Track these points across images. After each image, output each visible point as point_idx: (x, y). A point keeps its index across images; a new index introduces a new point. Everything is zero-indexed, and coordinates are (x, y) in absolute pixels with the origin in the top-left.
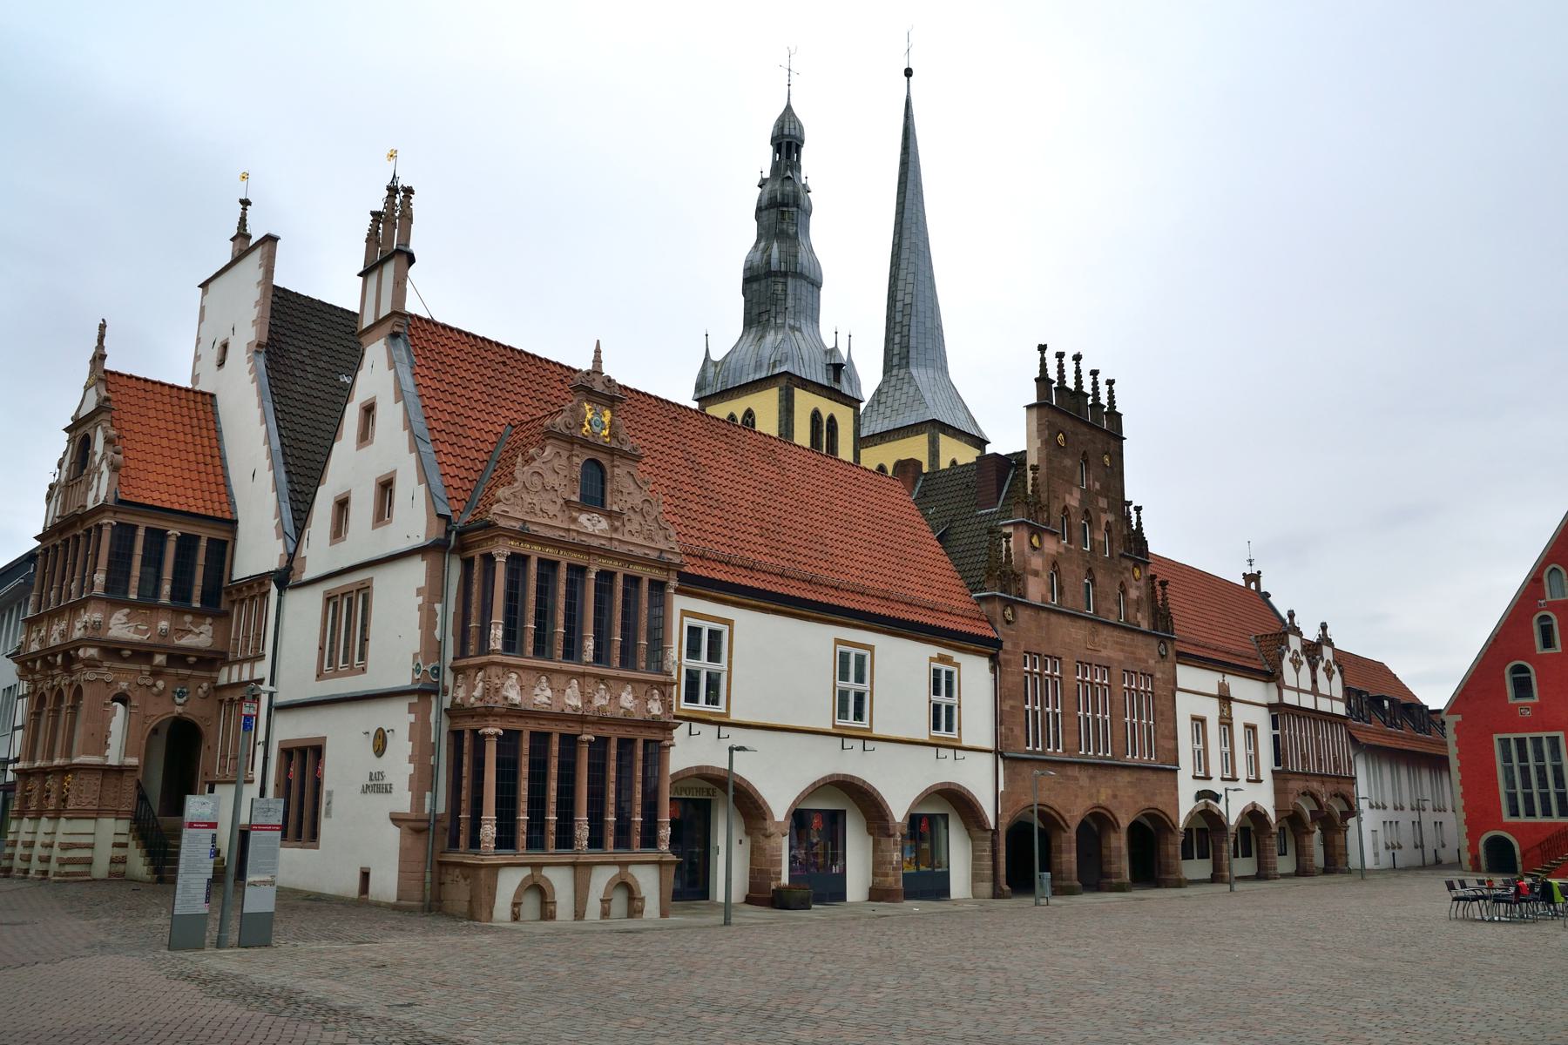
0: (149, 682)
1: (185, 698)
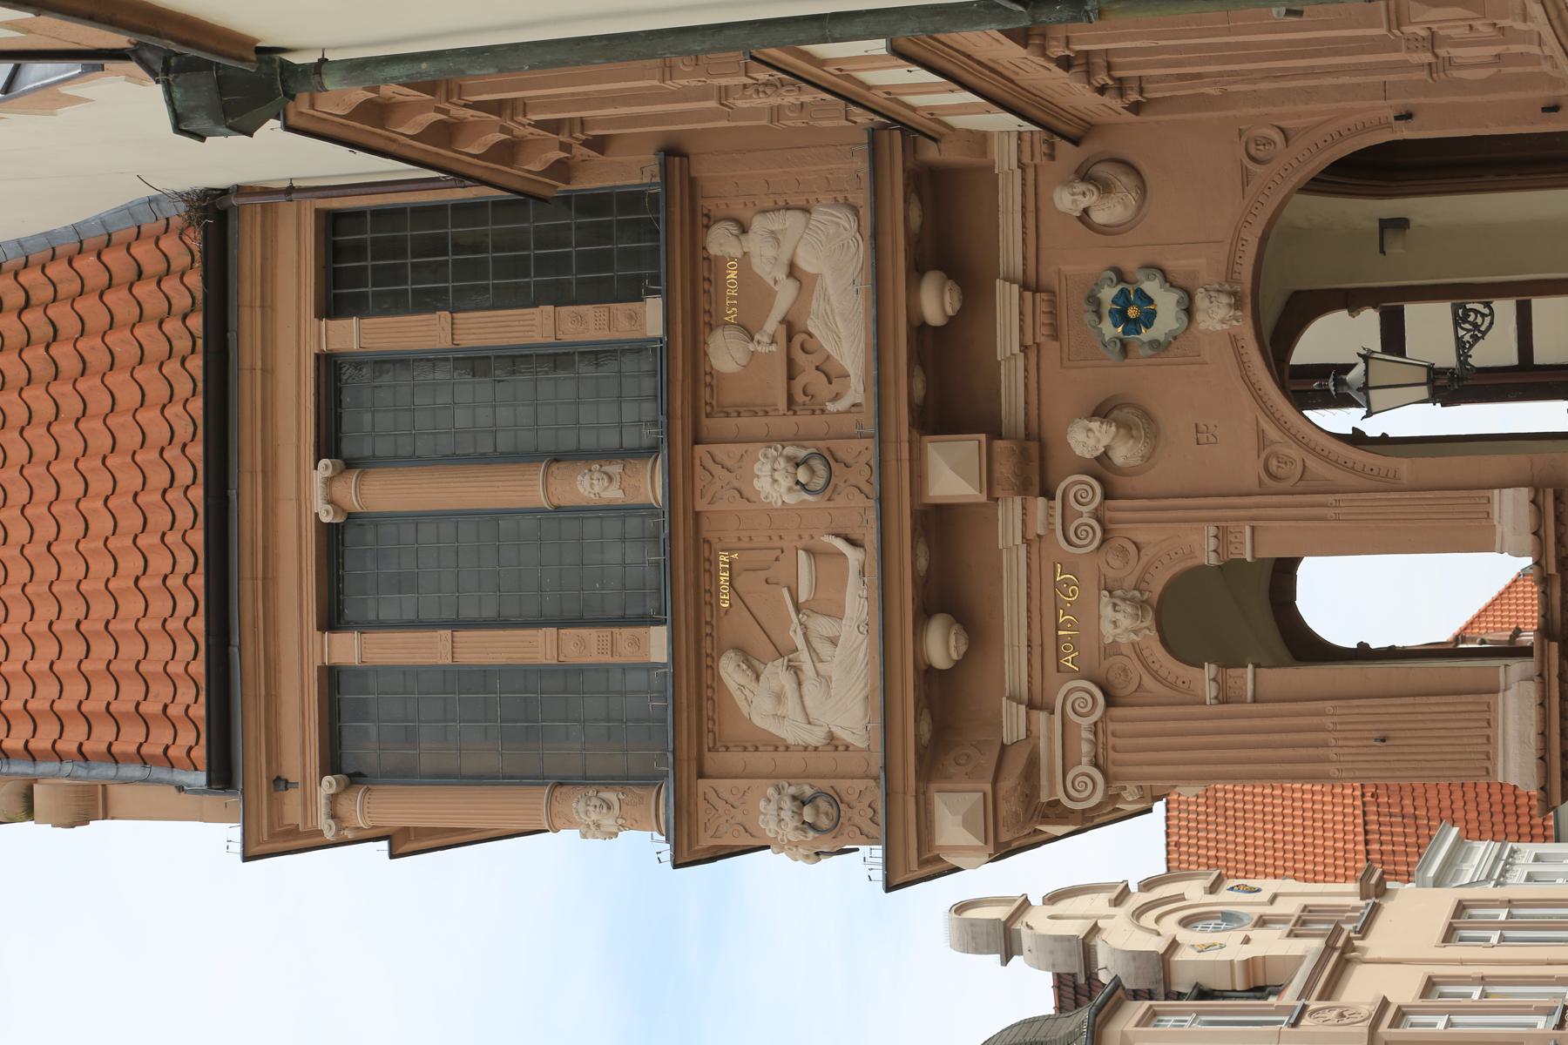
0: (1082, 492)
1: (1152, 287)
